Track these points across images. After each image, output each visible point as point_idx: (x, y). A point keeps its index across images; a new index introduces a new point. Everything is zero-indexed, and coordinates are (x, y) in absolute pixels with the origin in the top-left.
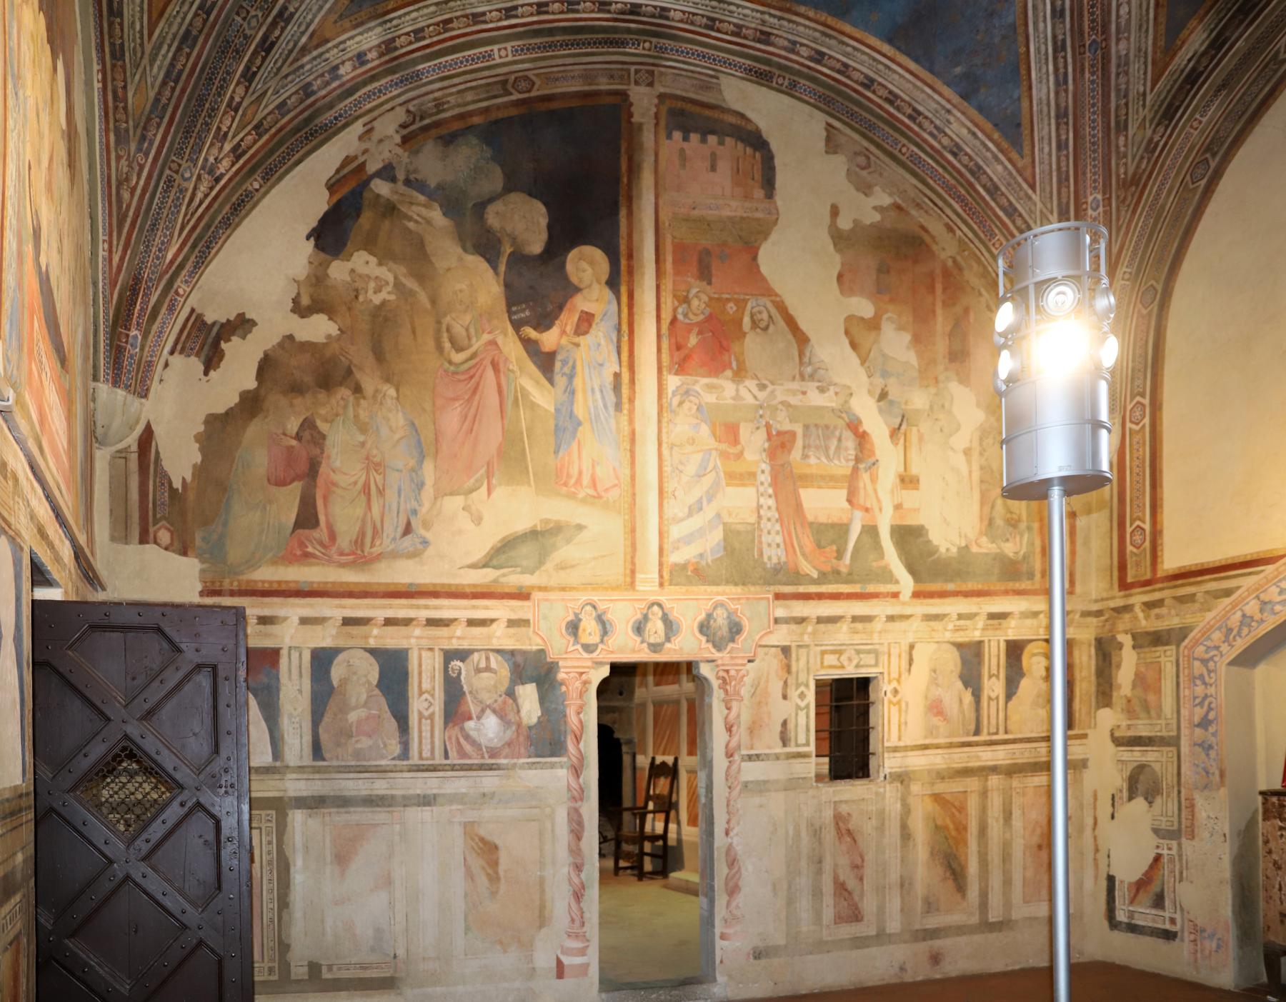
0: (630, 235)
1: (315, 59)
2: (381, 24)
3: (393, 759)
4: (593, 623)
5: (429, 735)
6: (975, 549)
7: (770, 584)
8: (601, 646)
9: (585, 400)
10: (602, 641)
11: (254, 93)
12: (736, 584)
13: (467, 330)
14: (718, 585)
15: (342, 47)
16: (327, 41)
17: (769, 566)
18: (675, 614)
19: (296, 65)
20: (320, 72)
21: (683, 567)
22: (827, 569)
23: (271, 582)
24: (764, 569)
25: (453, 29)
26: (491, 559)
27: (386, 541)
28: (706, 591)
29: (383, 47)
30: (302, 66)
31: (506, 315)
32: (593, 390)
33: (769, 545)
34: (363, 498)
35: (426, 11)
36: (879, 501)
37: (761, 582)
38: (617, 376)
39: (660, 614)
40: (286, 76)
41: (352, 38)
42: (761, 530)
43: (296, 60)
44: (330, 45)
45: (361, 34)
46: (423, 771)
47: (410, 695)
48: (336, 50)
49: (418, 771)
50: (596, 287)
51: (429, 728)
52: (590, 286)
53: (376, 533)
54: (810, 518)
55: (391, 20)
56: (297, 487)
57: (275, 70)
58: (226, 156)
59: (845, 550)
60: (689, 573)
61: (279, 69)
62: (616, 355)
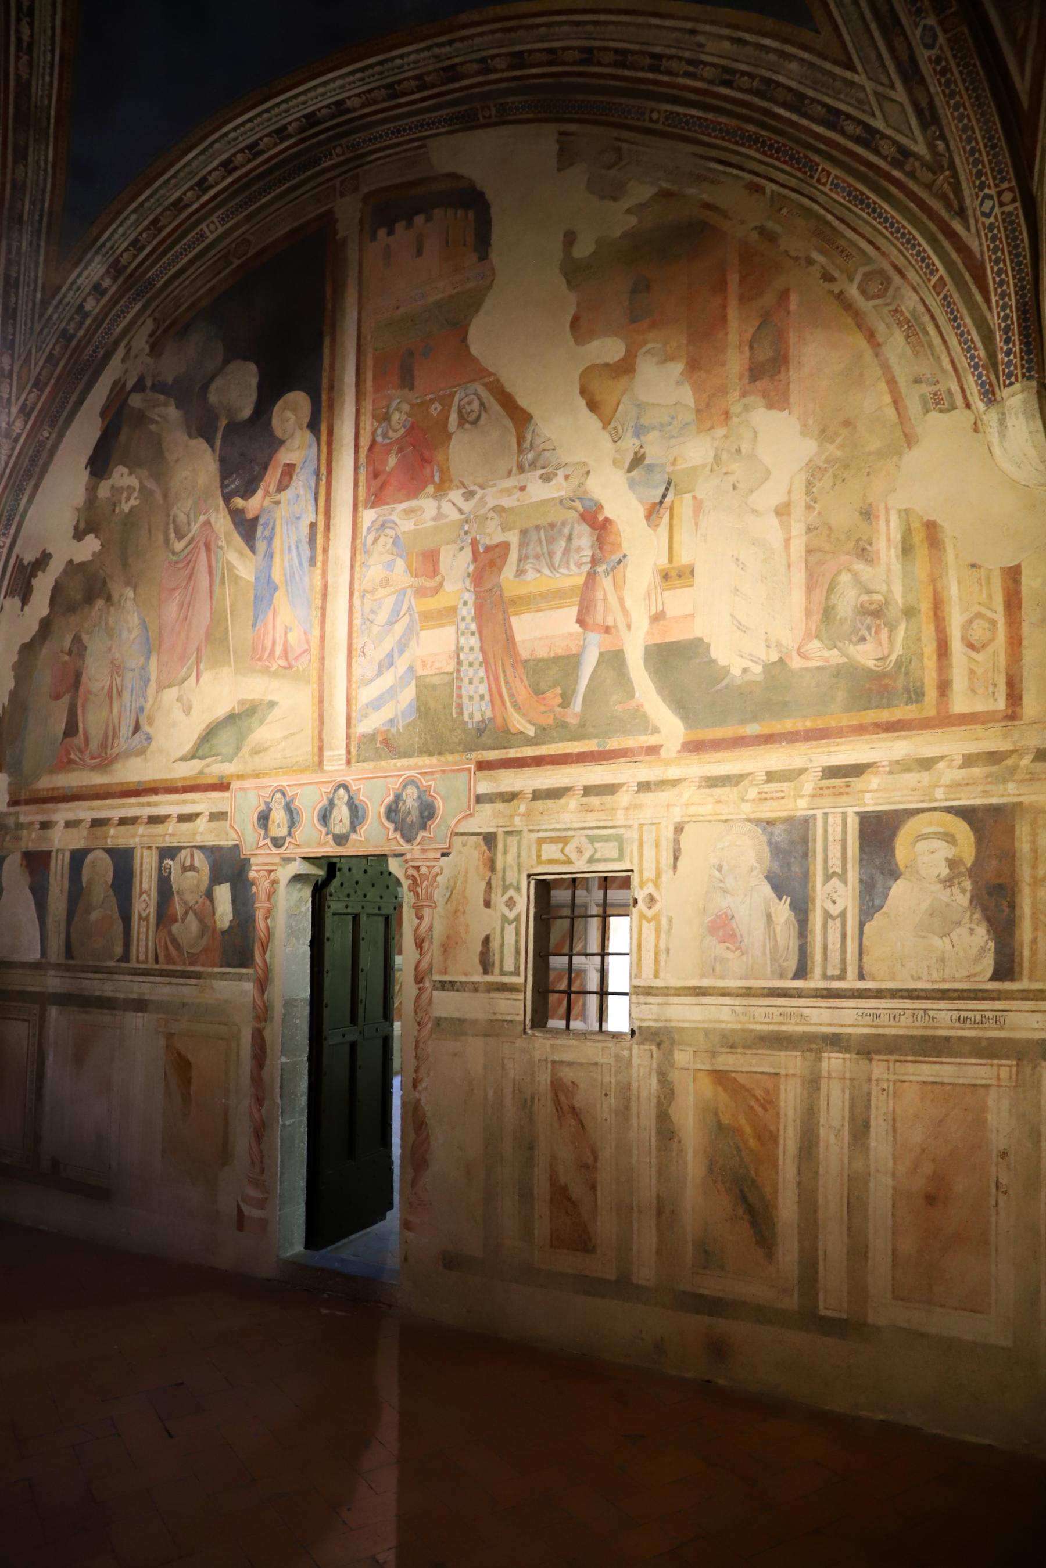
0: (332, 365)
1: (57, 307)
2: (97, 252)
4: (282, 812)
6: (796, 663)
7: (471, 750)
8: (288, 840)
9: (282, 560)
10: (290, 834)
11: (19, 357)
12: (431, 755)
13: (188, 516)
14: (410, 757)
15: (75, 287)
16: (60, 288)
17: (470, 726)
18: (361, 797)
19: (43, 320)
20: (68, 316)
21: (372, 737)
22: (549, 720)
23: (48, 790)
24: (465, 731)
25: (165, 226)
26: (197, 750)
27: (122, 740)
28: (395, 765)
29: (112, 270)
30: (50, 318)
31: (219, 490)
32: (289, 548)
33: (471, 698)
34: (107, 701)
35: (129, 222)
36: (625, 612)
37: (460, 749)
38: (313, 526)
39: (346, 798)
40: (41, 331)
41: (79, 276)
42: (461, 680)
43: (41, 315)
44: (64, 290)
45: (85, 268)
48: (72, 292)
50: (298, 433)
52: (292, 435)
53: (115, 734)
54: (524, 653)
55: (103, 245)
56: (67, 698)
57: (28, 331)
58: (16, 418)
59: (574, 691)
60: (378, 745)
61: (32, 328)
62: (313, 503)
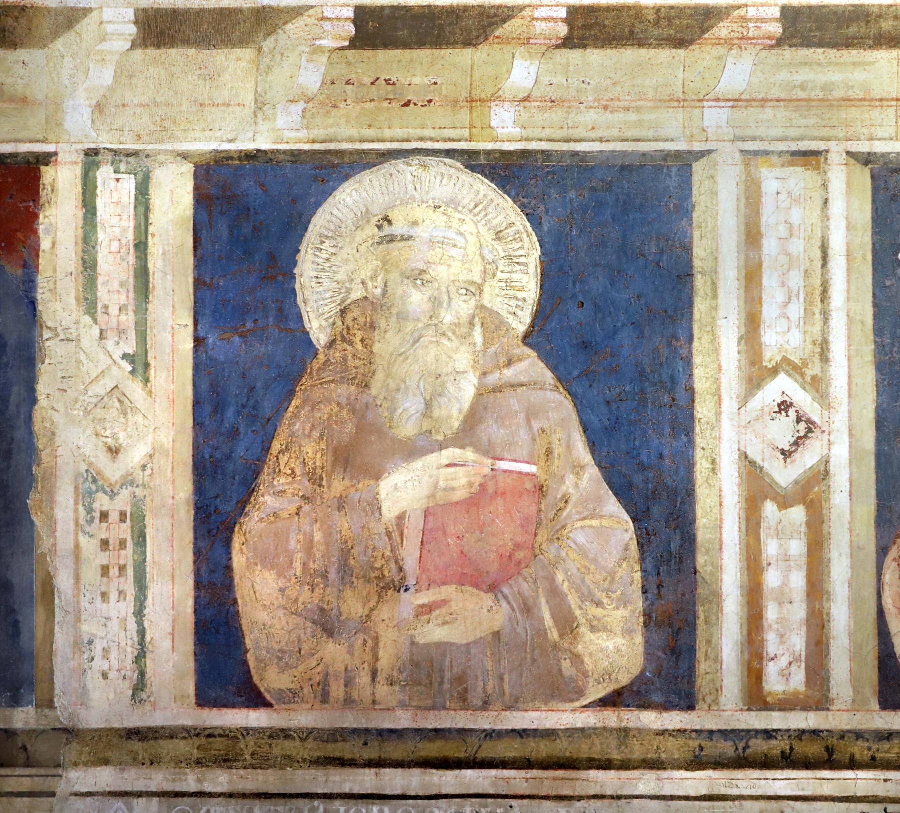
3: (613, 700)
5: (798, 581)
46: (766, 763)
47: (701, 382)
49: (742, 762)
51: (797, 547)
